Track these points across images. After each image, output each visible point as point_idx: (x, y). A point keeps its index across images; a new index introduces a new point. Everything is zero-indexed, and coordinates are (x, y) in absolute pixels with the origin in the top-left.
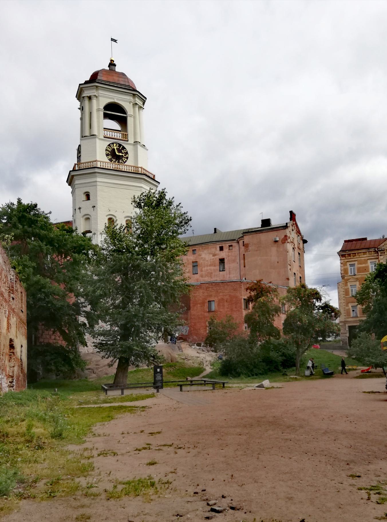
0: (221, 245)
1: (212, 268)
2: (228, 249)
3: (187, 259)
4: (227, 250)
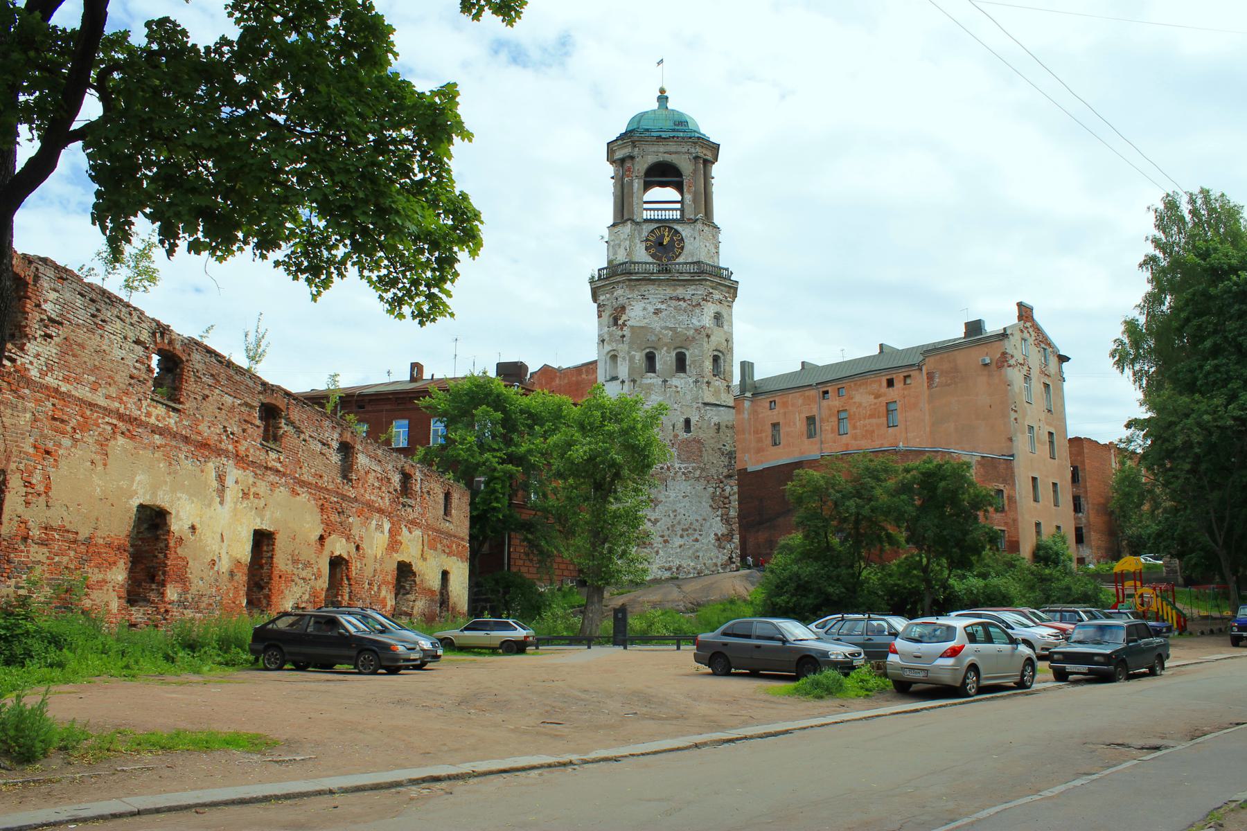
0: (889, 377)
1: (874, 421)
2: (903, 382)
3: (829, 405)
4: (901, 385)
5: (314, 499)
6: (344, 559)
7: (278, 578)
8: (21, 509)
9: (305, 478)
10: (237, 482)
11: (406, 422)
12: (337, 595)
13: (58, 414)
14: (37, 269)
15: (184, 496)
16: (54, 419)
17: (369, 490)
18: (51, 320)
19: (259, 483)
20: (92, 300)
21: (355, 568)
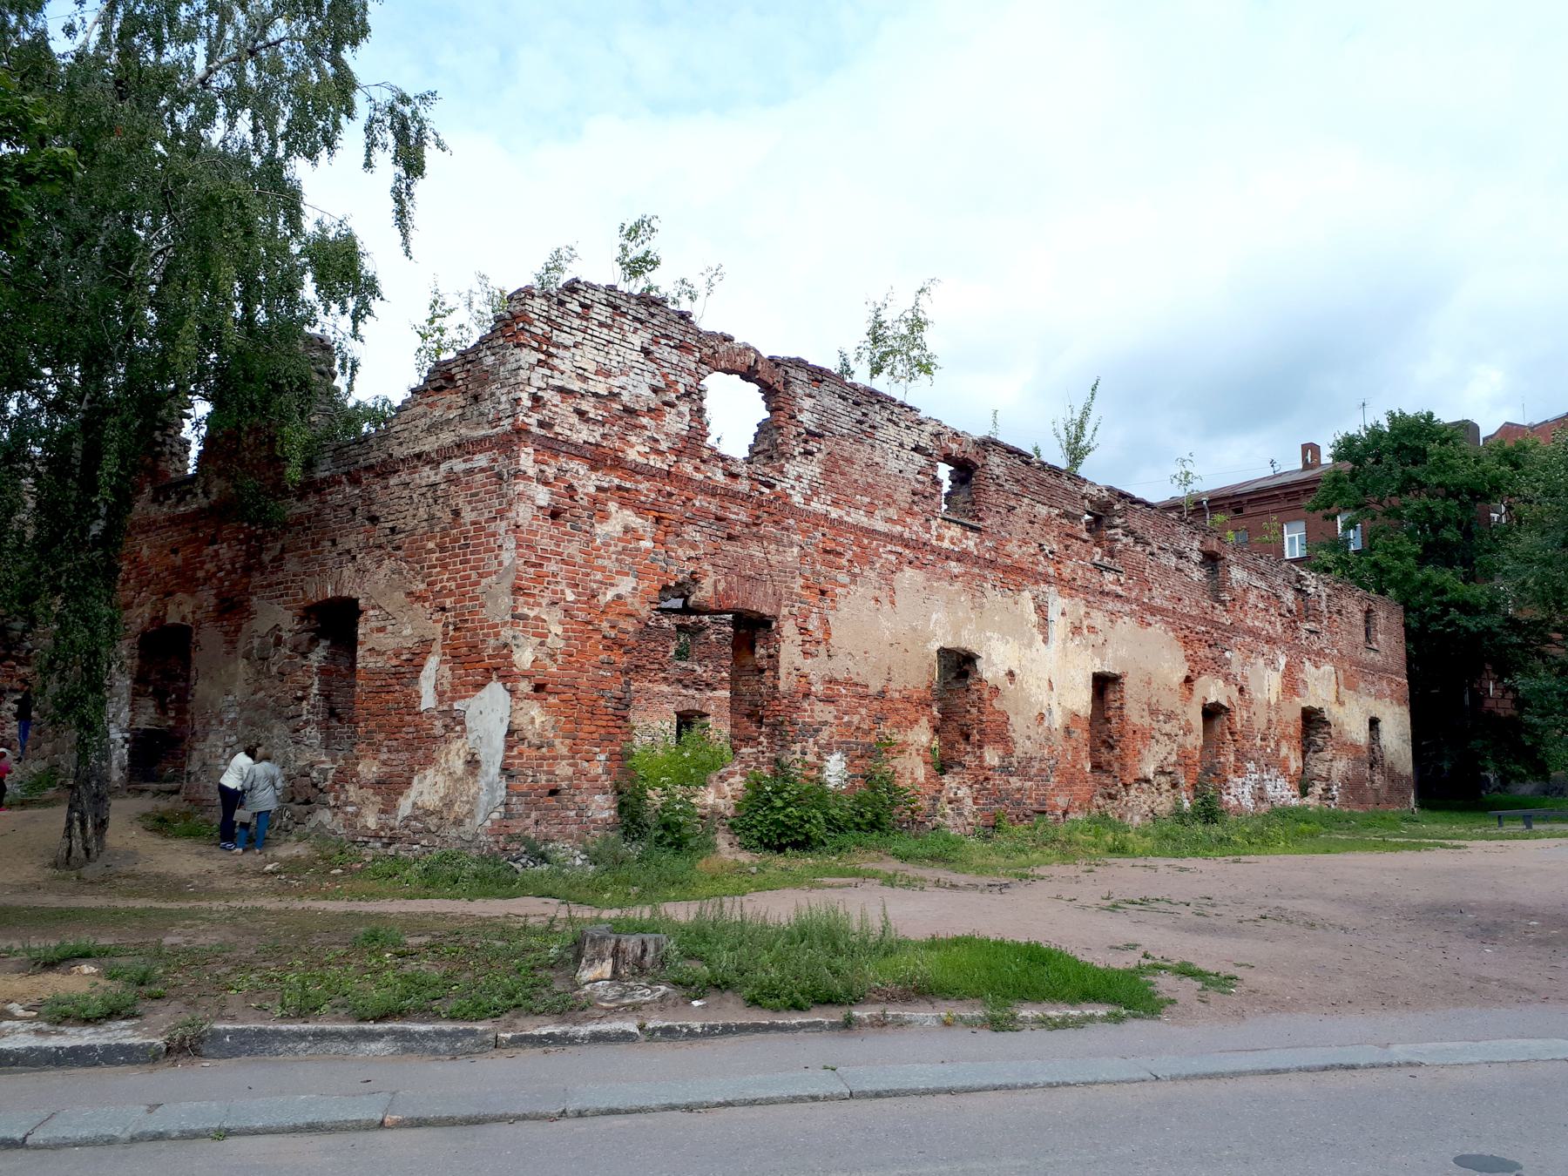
5: (1174, 630)
6: (1223, 707)
7: (1131, 734)
8: (799, 661)
9: (1158, 602)
10: (1063, 614)
11: (1302, 525)
12: (1218, 755)
13: (830, 546)
14: (787, 372)
15: (996, 636)
16: (826, 551)
17: (1251, 614)
18: (809, 432)
19: (1094, 613)
20: (857, 404)
21: (1240, 717)
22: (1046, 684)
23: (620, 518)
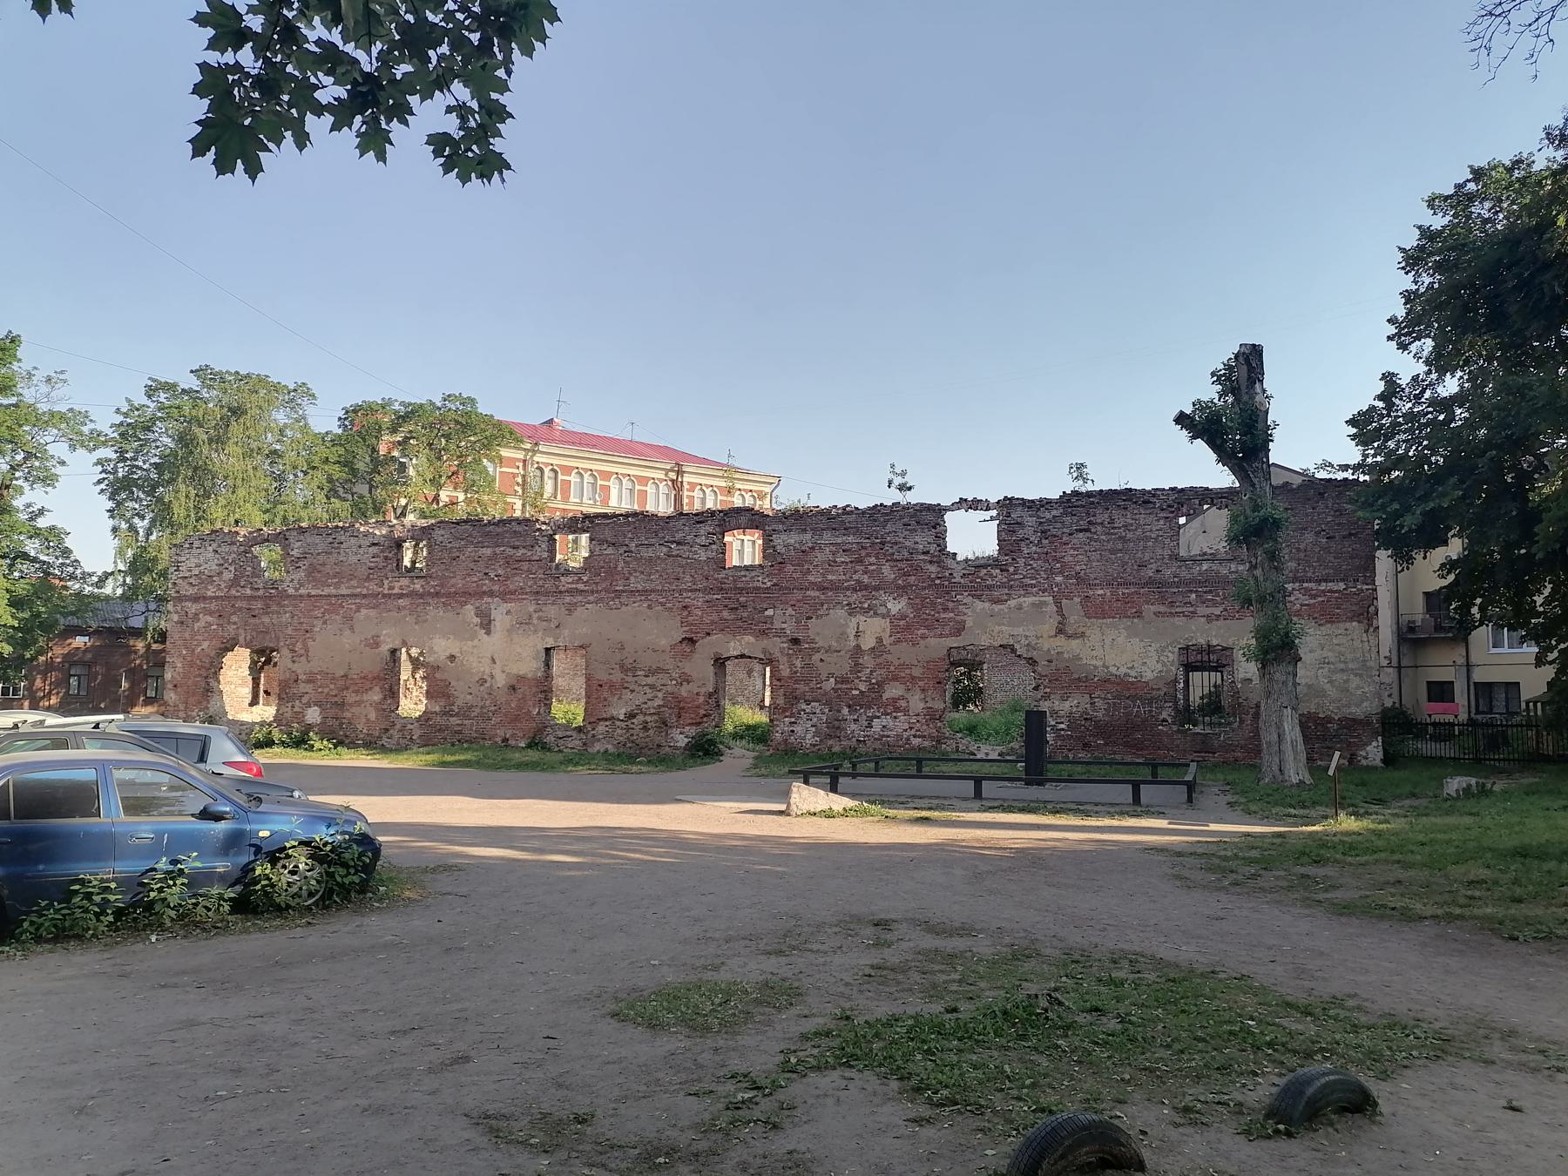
8: (290, 665)
22: (489, 661)
23: (205, 619)
